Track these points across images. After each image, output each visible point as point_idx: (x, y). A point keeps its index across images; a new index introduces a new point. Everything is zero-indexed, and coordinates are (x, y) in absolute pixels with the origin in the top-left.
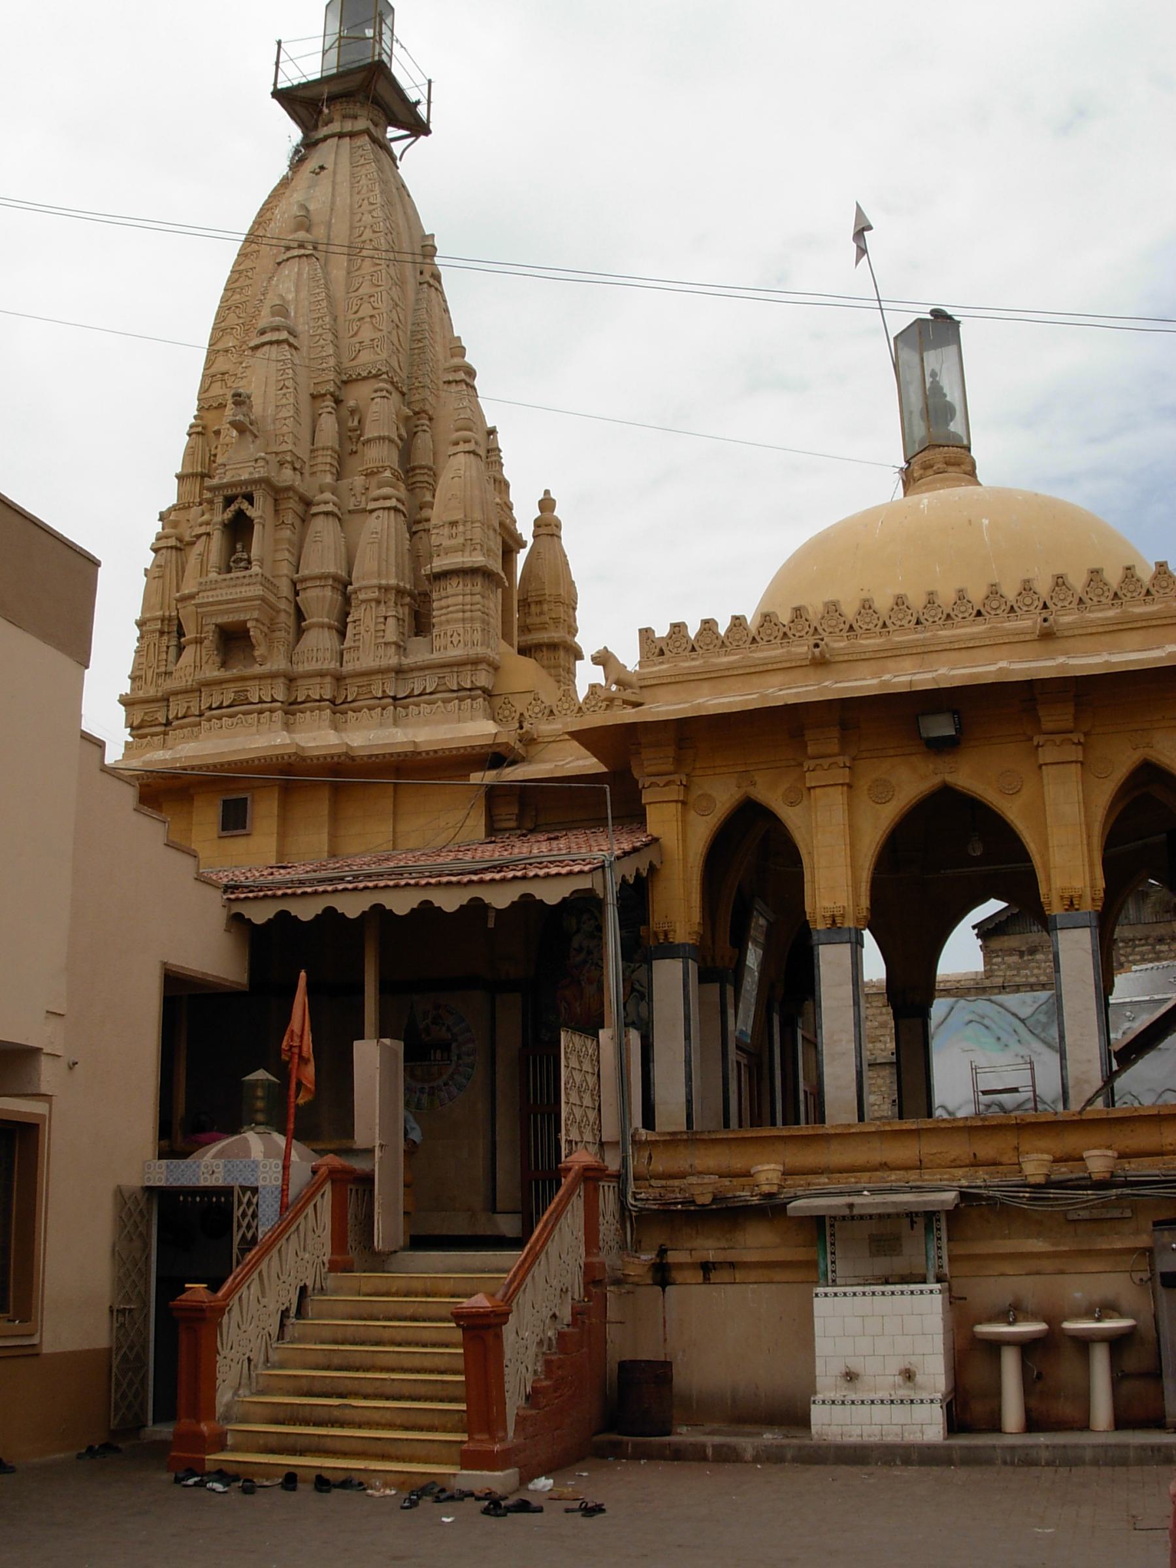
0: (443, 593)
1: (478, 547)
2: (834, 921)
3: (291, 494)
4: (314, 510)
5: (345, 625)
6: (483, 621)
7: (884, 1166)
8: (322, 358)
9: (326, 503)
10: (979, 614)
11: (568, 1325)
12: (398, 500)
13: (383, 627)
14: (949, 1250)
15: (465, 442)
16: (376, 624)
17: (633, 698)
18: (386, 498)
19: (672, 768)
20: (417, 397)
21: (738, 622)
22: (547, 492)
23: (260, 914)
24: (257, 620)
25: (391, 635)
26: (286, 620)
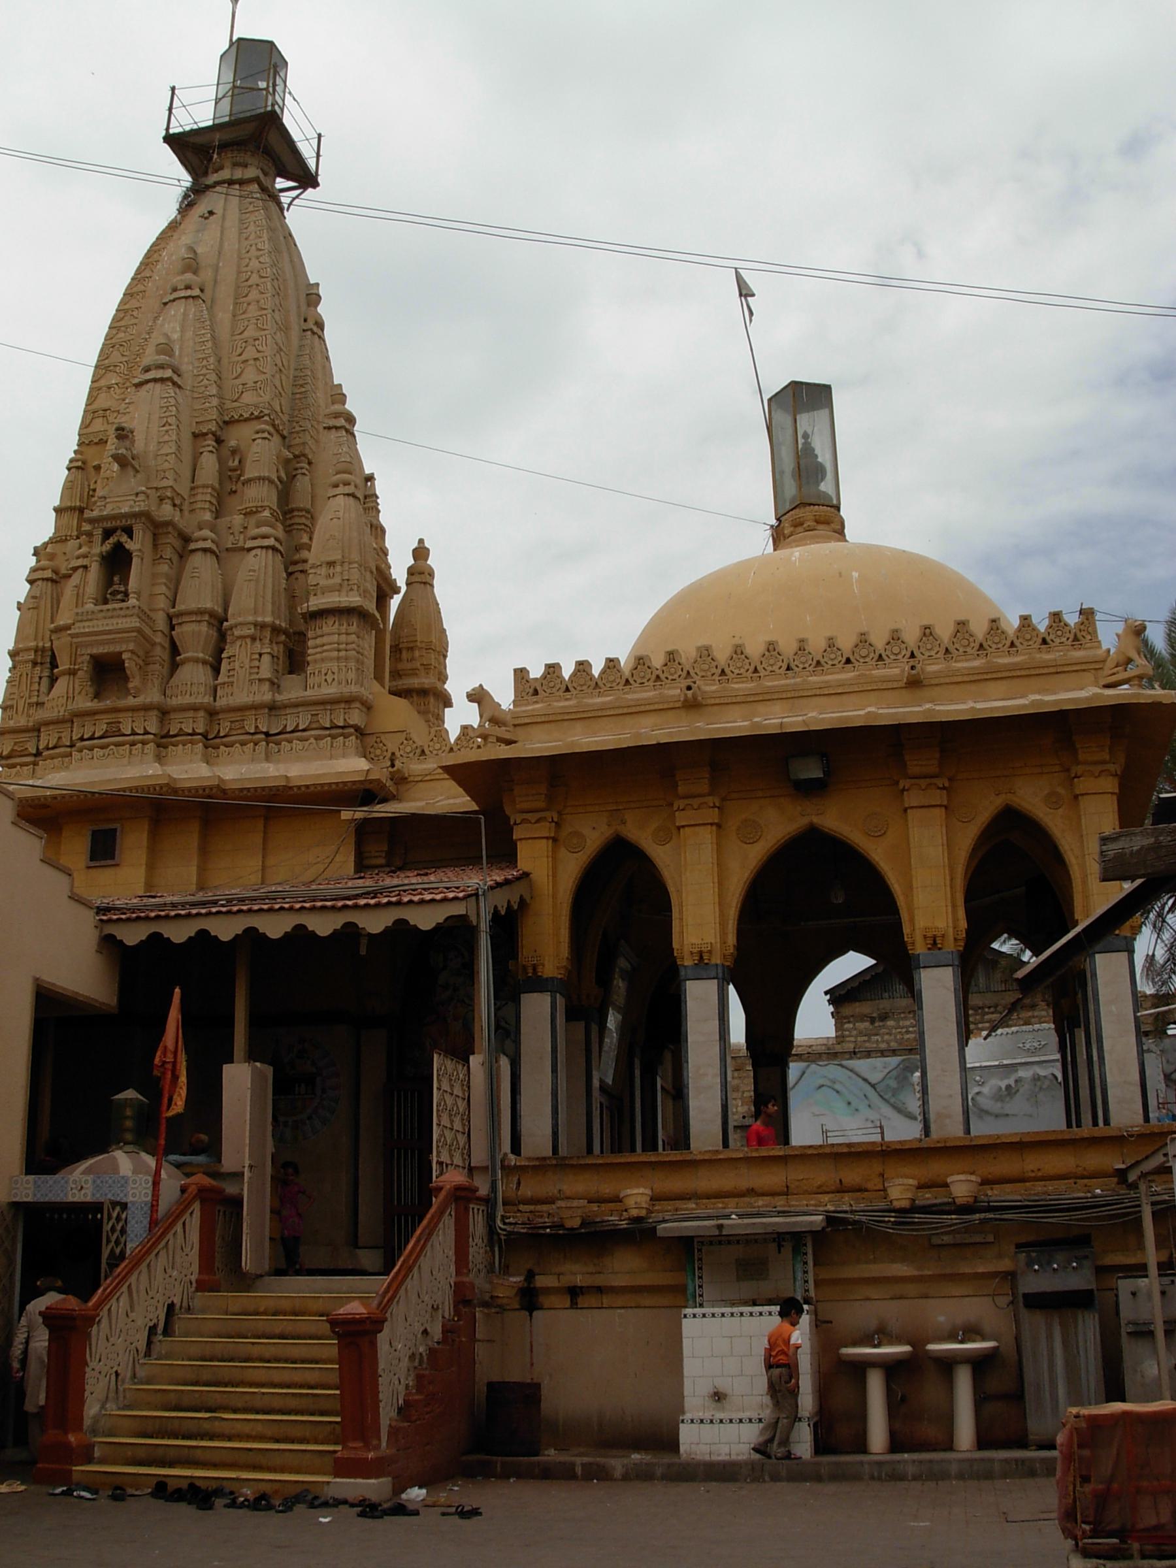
0: (319, 632)
2: (701, 958)
3: (170, 529)
4: (193, 546)
6: (358, 661)
7: (752, 1192)
9: (205, 540)
10: (848, 661)
11: (438, 1343)
12: (276, 539)
13: (256, 663)
14: (815, 1275)
15: (345, 484)
16: (251, 660)
17: (508, 736)
18: (264, 537)
20: (297, 441)
21: (611, 664)
22: (421, 541)
23: (132, 936)
24: (132, 652)
25: (266, 671)
26: (161, 653)
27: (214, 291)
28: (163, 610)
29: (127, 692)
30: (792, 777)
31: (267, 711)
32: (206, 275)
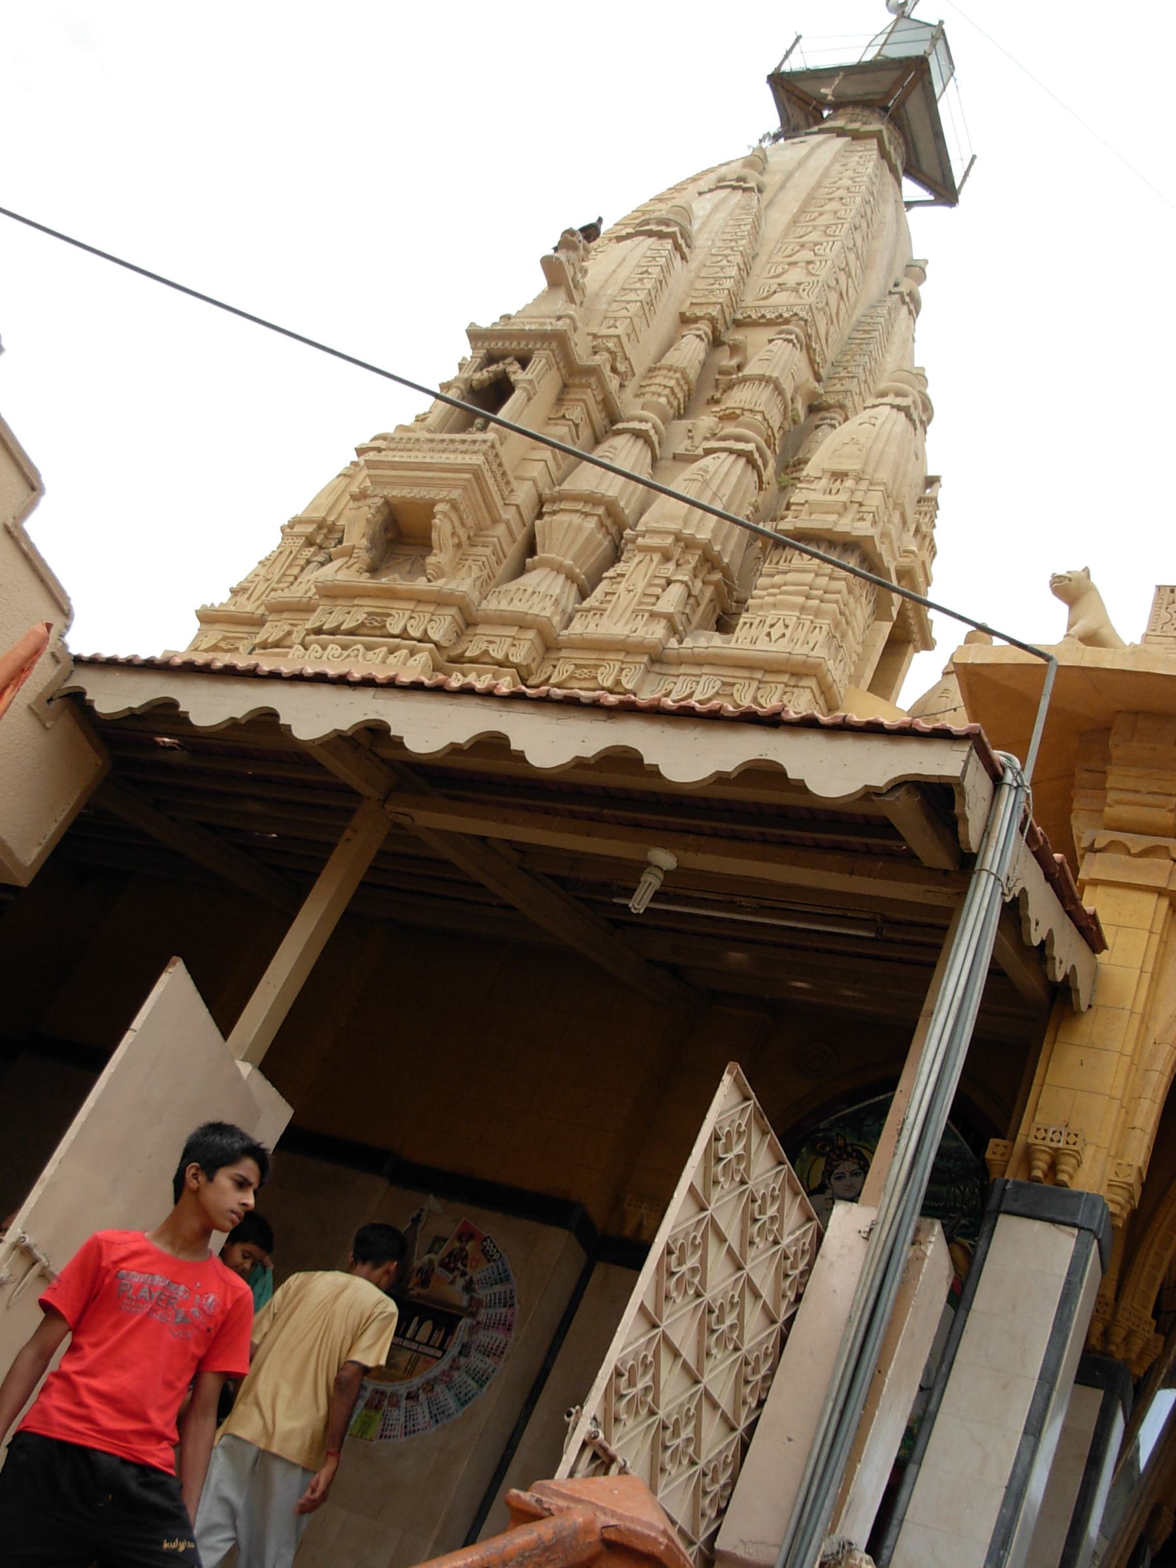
3: (593, 380)
4: (620, 426)
5: (596, 580)
6: (837, 625)
13: (659, 591)
15: (897, 395)
16: (650, 585)
18: (739, 439)
20: (838, 387)
24: (454, 505)
25: (672, 600)
26: (503, 538)
27: (775, 195)
31: (645, 659)
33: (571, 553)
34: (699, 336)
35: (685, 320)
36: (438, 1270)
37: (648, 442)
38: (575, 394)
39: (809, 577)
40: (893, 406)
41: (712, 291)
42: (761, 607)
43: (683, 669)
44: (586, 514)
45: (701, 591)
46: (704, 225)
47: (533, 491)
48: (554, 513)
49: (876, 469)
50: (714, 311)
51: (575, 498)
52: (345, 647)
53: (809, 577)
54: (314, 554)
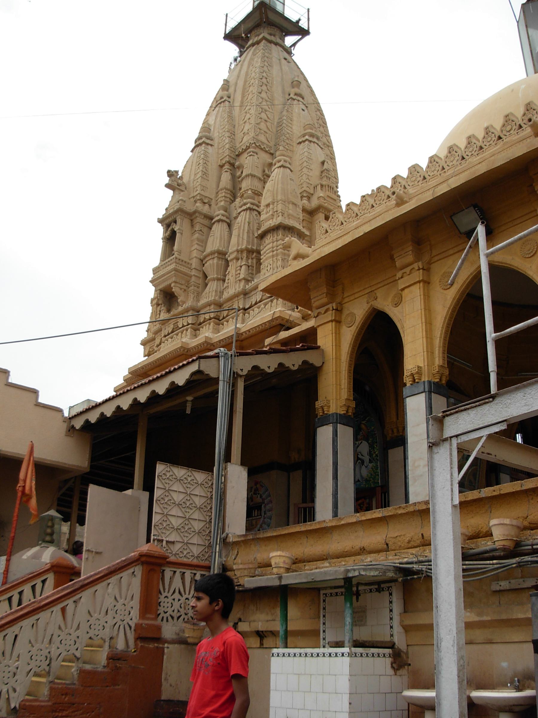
1: (280, 214)
3: (197, 214)
7: (363, 551)
8: (224, 146)
9: (218, 215)
10: (500, 138)
11: (104, 667)
13: (239, 272)
14: (401, 622)
16: (236, 271)
19: (325, 300)
23: (78, 424)
24: (175, 282)
27: (234, 95)
28: (196, 257)
29: (178, 305)
30: (463, 230)
31: (242, 296)
32: (231, 90)
33: (215, 273)
34: (226, 171)
35: (221, 166)
36: (254, 496)
37: (223, 221)
38: (195, 221)
39: (271, 245)
40: (278, 167)
41: (224, 152)
42: (266, 259)
43: (253, 293)
44: (213, 258)
45: (252, 262)
46: (214, 127)
47: (198, 260)
48: (206, 263)
49: (277, 197)
50: (227, 159)
51: (208, 255)
52: (172, 338)
53: (271, 245)
54: (161, 308)
